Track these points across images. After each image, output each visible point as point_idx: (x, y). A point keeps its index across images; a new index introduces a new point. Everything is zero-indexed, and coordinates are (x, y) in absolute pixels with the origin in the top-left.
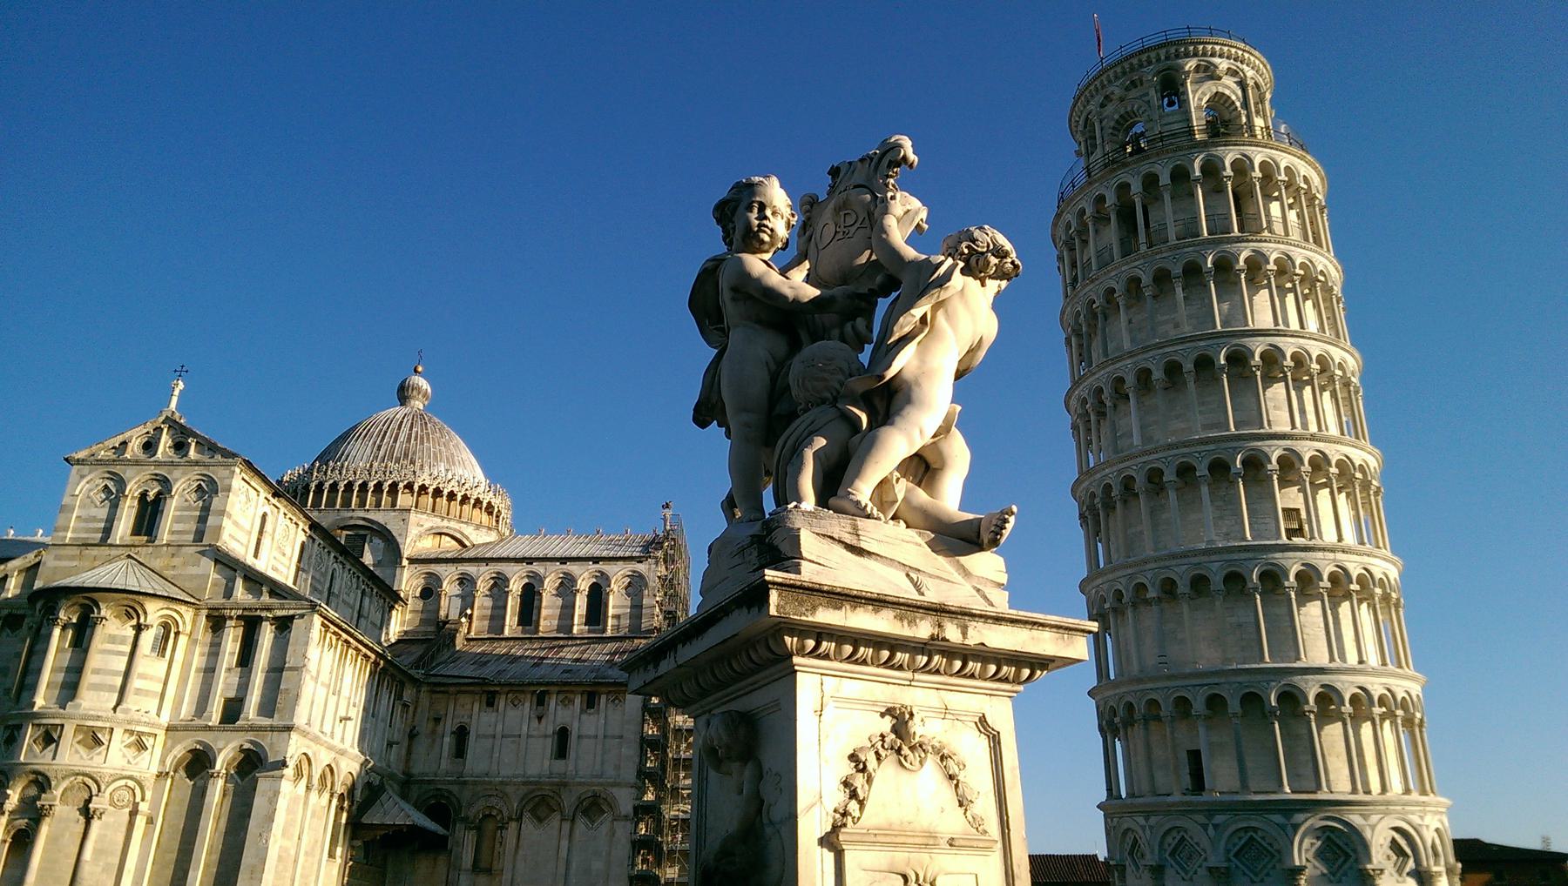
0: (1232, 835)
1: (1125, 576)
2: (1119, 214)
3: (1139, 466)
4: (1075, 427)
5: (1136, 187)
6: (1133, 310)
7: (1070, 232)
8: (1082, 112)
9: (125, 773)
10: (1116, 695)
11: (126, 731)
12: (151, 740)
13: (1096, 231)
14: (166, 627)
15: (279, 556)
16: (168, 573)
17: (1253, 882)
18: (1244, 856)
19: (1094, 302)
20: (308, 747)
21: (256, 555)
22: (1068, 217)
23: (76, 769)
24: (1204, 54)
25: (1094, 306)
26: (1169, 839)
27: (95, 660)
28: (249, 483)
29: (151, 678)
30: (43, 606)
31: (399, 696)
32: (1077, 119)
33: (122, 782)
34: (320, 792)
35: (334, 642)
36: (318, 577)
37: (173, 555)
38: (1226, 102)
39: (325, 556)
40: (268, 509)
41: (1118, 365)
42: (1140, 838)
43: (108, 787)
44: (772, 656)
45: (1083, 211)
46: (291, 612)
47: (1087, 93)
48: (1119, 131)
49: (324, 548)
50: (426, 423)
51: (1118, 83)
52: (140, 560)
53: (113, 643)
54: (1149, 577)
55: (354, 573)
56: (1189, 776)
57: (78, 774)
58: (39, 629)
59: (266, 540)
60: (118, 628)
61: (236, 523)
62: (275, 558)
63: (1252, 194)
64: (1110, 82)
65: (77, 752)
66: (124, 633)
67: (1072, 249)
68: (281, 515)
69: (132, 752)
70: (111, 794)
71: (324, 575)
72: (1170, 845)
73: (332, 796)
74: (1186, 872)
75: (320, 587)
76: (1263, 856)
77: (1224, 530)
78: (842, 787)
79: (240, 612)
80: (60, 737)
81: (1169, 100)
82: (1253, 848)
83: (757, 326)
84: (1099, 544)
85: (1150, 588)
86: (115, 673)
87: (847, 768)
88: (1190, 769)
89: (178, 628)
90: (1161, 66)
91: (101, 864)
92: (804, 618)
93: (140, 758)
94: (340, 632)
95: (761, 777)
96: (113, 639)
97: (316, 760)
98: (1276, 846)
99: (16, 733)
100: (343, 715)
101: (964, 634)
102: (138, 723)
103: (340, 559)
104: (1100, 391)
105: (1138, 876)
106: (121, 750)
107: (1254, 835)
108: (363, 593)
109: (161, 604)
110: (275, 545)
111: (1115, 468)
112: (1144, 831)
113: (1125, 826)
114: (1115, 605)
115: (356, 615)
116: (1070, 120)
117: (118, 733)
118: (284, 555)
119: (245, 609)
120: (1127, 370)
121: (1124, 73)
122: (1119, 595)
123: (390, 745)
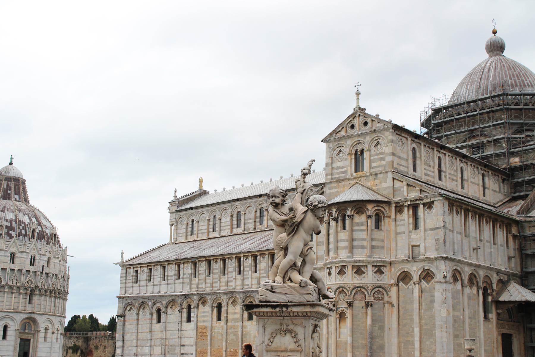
9: (377, 285)
11: (373, 266)
12: (385, 268)
14: (377, 215)
15: (427, 168)
16: (375, 188)
20: (457, 266)
21: (415, 170)
23: (357, 285)
27: (357, 235)
28: (401, 135)
29: (378, 240)
30: (328, 212)
31: (509, 231)
33: (377, 289)
34: (471, 287)
35: (459, 211)
36: (452, 172)
37: (375, 179)
39: (454, 161)
40: (414, 145)
43: (371, 292)
46: (432, 200)
49: (452, 157)
50: (503, 65)
52: (362, 184)
53: (358, 226)
55: (474, 166)
57: (358, 287)
58: (329, 223)
59: (418, 162)
60: (358, 219)
61: (399, 157)
62: (425, 169)
65: (355, 277)
66: (361, 221)
68: (422, 146)
69: (377, 276)
70: (373, 295)
71: (456, 171)
73: (478, 288)
75: (454, 178)
79: (409, 203)
80: (347, 271)
83: (277, 227)
86: (364, 240)
87: (269, 336)
89: (384, 215)
91: (377, 326)
93: (382, 277)
94: (461, 205)
96: (358, 224)
97: (463, 272)
99: (331, 270)
100: (475, 247)
102: (377, 261)
103: (464, 160)
106: (372, 275)
108: (483, 175)
109: (374, 205)
110: (423, 162)
115: (481, 189)
117: (370, 267)
118: (430, 166)
119: (411, 201)
123: (510, 258)
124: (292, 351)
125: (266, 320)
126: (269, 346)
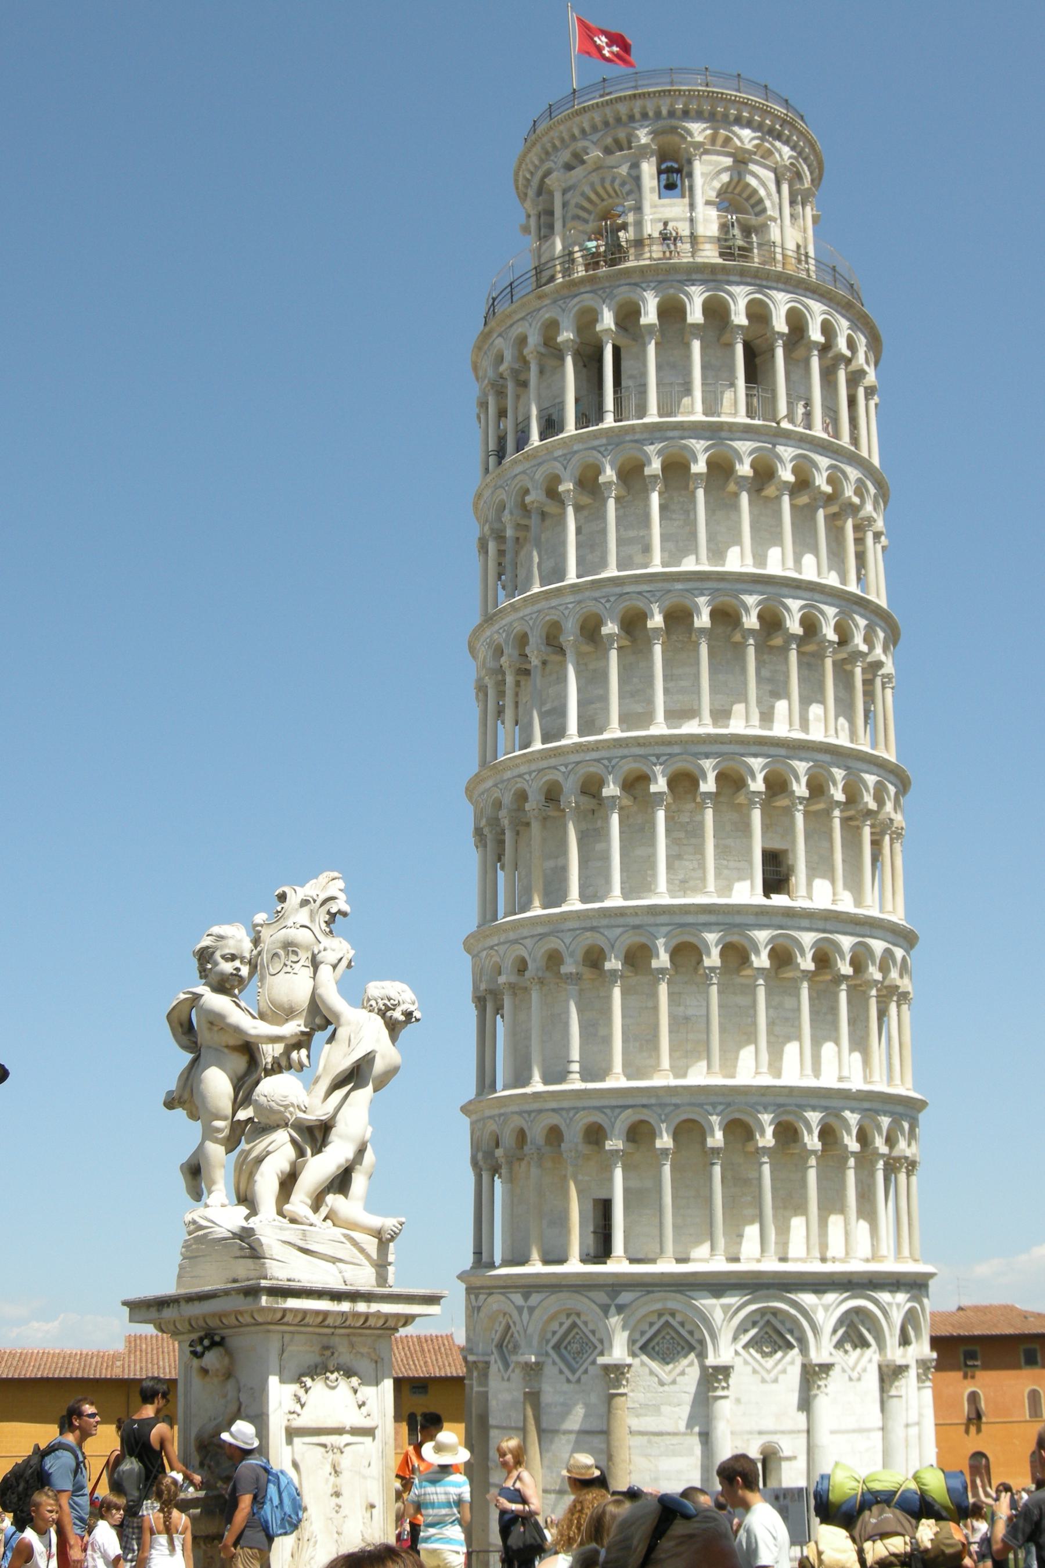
0: (639, 1321)
1: (532, 936)
2: (578, 356)
3: (570, 767)
4: (481, 689)
5: (608, 320)
6: (585, 513)
7: (502, 368)
8: (537, 167)
10: (500, 1115)
13: (541, 372)
17: (662, 1384)
18: (653, 1348)
19: (527, 492)
22: (503, 345)
24: (725, 116)
25: (528, 499)
26: (555, 1326)
32: (528, 176)
38: (750, 197)
41: (554, 602)
42: (514, 1323)
44: (253, 1321)
45: (522, 341)
47: (545, 139)
48: (589, 212)
51: (595, 137)
54: (568, 941)
56: (592, 1236)
63: (772, 351)
64: (583, 131)
67: (501, 394)
72: (554, 1333)
74: (573, 1371)
76: (679, 1348)
77: (681, 877)
78: (293, 1397)
81: (668, 179)
82: (668, 1337)
84: (501, 874)
85: (568, 960)
88: (596, 1226)
90: (661, 124)
92: (280, 1306)
95: (239, 1390)
98: (697, 1336)
101: (369, 1307)
104: (523, 640)
105: (506, 1377)
107: (671, 1320)
111: (534, 767)
112: (520, 1313)
113: (495, 1307)
114: (513, 979)
116: (517, 174)
120: (566, 612)
121: (606, 124)
122: (522, 967)
124: (356, 1431)
125: (287, 1337)
126: (295, 1416)
